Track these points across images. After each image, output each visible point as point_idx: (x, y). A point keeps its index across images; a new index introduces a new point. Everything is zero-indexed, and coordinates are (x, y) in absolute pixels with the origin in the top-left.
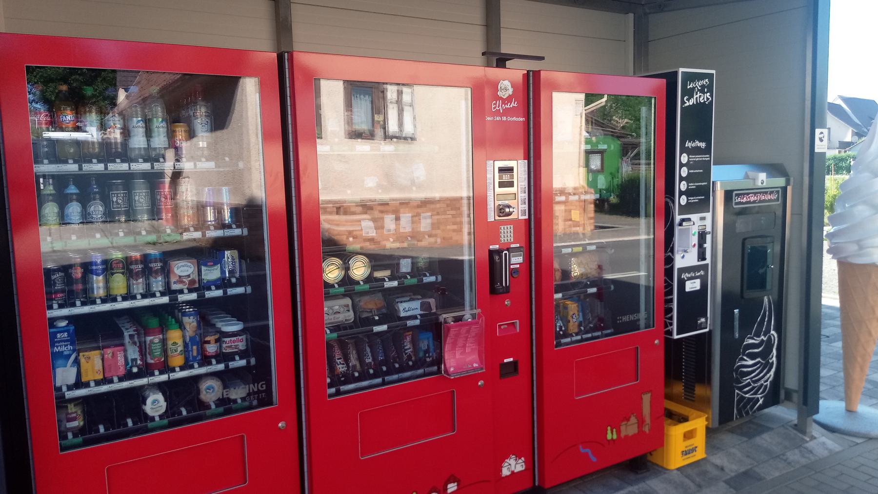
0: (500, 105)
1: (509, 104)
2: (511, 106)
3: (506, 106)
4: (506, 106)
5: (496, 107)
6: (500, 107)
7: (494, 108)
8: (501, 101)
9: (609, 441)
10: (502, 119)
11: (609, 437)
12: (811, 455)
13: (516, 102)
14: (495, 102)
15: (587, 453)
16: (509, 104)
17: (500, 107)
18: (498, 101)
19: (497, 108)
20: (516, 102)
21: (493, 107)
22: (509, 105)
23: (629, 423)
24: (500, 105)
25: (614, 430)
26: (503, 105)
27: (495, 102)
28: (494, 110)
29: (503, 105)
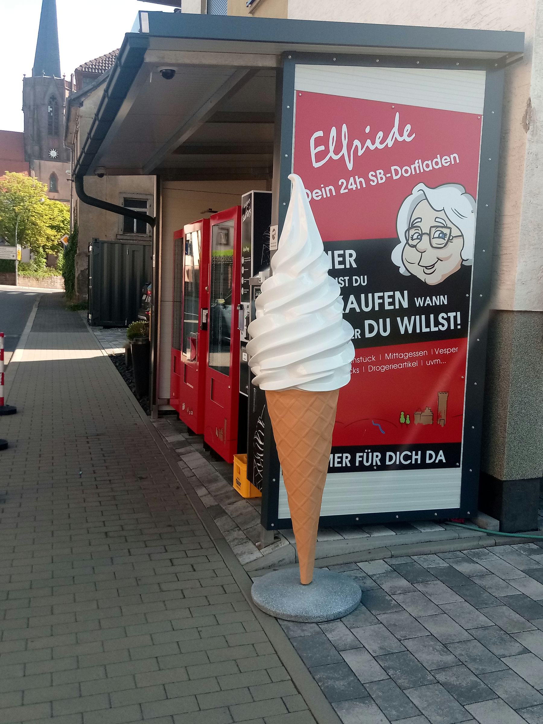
0: (345, 143)
1: (381, 134)
2: (390, 142)
3: (368, 143)
4: (368, 143)
5: (327, 151)
6: (344, 151)
7: (320, 156)
8: (344, 128)
9: (402, 424)
10: (368, 181)
11: (402, 420)
12: (199, 282)
13: (408, 127)
14: (320, 134)
15: (375, 423)
16: (381, 134)
17: (344, 151)
18: (333, 132)
19: (331, 154)
20: (408, 127)
21: (313, 152)
22: (378, 141)
23: (423, 414)
24: (345, 143)
25: (408, 416)
26: (357, 142)
27: (320, 134)
28: (316, 165)
29: (357, 142)
